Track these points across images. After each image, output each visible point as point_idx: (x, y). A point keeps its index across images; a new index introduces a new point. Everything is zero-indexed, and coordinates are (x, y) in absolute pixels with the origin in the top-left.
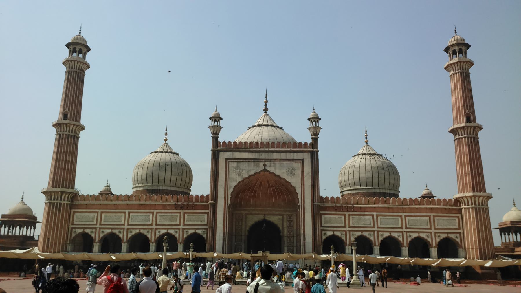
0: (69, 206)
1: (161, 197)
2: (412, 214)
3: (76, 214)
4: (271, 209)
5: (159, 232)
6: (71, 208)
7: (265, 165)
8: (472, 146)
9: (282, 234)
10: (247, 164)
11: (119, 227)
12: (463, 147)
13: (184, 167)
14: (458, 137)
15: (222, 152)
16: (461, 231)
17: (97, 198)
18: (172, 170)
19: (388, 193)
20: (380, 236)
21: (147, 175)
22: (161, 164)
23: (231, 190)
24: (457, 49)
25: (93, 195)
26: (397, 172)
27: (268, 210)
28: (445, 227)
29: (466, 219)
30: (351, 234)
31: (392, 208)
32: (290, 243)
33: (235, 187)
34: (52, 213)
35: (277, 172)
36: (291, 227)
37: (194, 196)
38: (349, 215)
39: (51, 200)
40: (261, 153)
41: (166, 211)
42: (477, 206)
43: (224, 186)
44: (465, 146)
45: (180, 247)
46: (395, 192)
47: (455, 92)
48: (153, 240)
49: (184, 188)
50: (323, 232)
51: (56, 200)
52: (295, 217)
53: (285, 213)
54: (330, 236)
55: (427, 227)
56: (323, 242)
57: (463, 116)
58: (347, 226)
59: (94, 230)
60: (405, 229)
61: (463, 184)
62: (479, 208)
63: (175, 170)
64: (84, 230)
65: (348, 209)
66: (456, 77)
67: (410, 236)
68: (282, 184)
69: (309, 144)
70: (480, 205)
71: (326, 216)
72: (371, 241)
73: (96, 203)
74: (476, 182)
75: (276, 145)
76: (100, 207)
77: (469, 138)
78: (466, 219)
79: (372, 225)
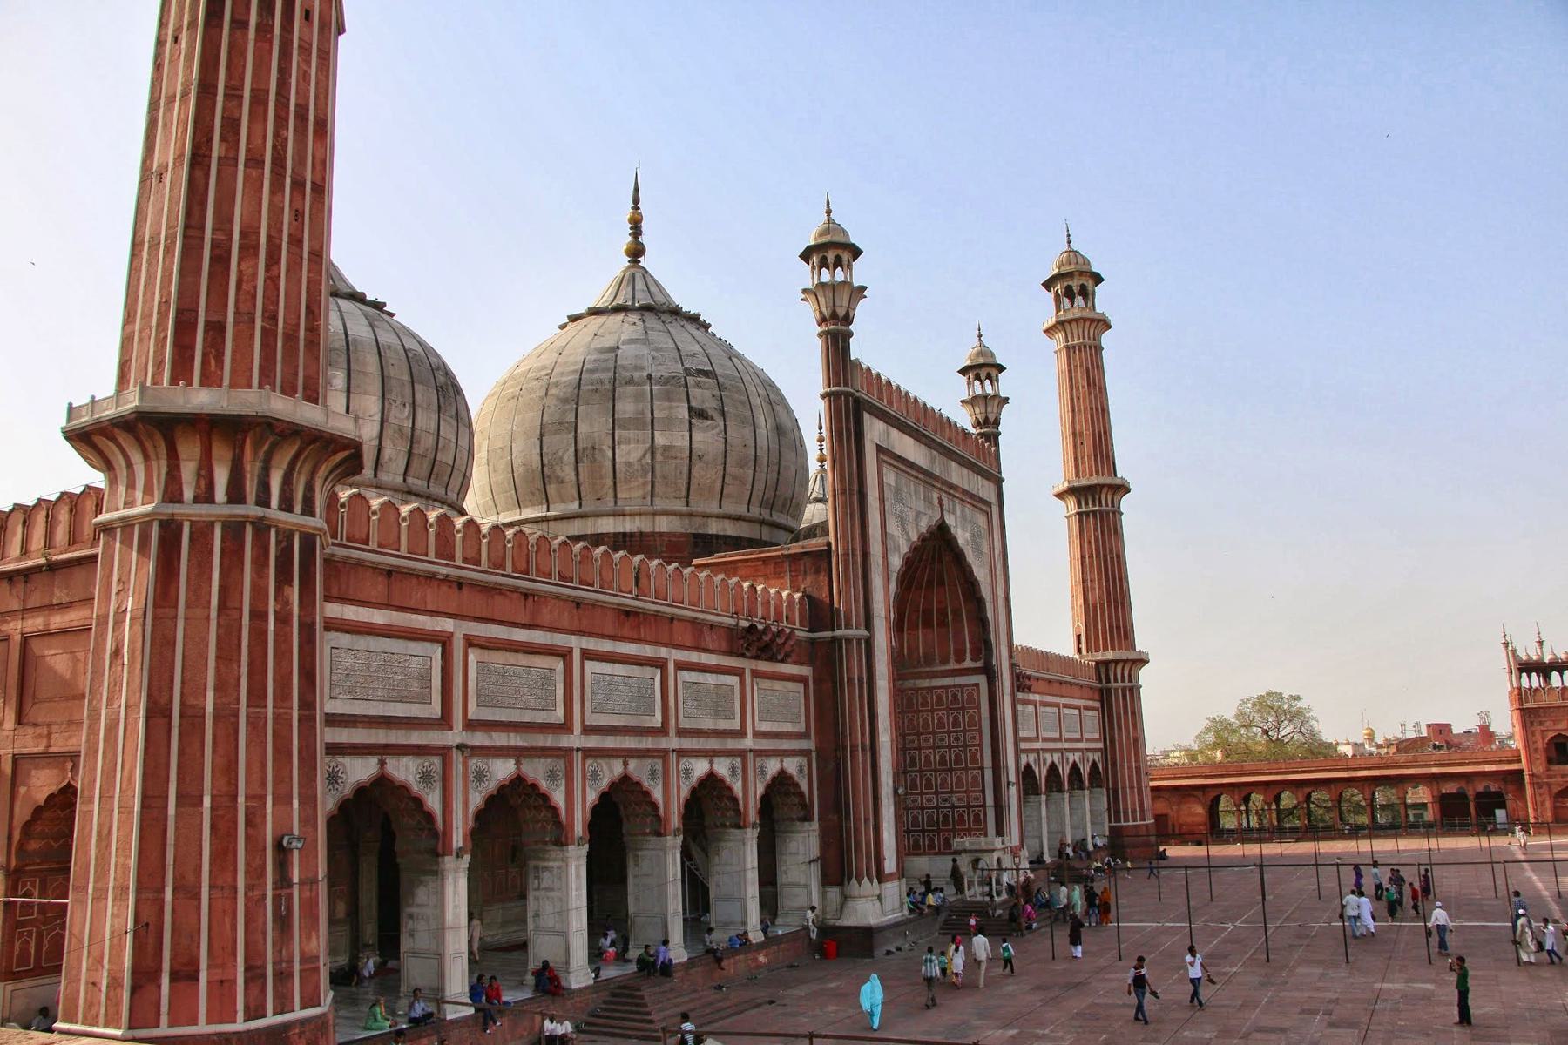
12: (1110, 535)
16: (1100, 745)
17: (438, 535)
21: (382, 422)
23: (893, 586)
24: (1089, 284)
34: (283, 619)
39: (267, 504)
40: (935, 453)
47: (1090, 394)
51: (298, 508)
59: (437, 761)
64: (382, 763)
66: (1091, 355)
73: (443, 570)
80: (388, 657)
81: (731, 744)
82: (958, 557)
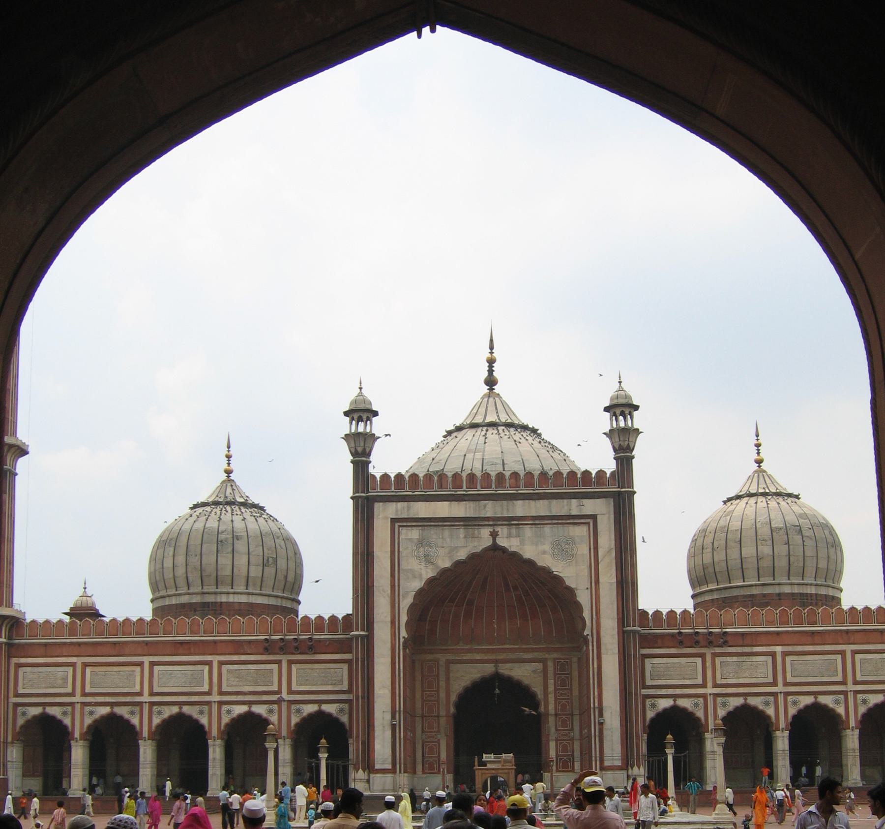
0: (5, 651)
1: (230, 623)
3: (21, 671)
4: (512, 646)
5: (229, 712)
6: (9, 657)
7: (494, 535)
9: (542, 709)
10: (447, 532)
11: (128, 699)
13: (280, 542)
15: (381, 504)
18: (250, 551)
19: (811, 595)
20: (789, 704)
21: (186, 565)
22: (222, 537)
23: (406, 602)
25: (60, 622)
26: (837, 539)
27: (506, 648)
30: (718, 702)
32: (564, 730)
33: (420, 593)
35: (528, 552)
36: (566, 691)
37: (313, 619)
38: (715, 655)
41: (243, 658)
43: (389, 592)
45: (284, 748)
46: (831, 592)
48: (215, 732)
49: (282, 598)
50: (648, 702)
52: (575, 666)
53: (549, 657)
54: (665, 710)
56: (650, 726)
58: (710, 684)
59: (69, 708)
60: (854, 684)
63: (257, 551)
64: (44, 709)
65: (710, 640)
67: (864, 702)
71: (656, 660)
72: (769, 717)
75: (522, 483)
76: (79, 649)
79: (770, 680)
80: (47, 673)
81: (265, 698)
82: (530, 563)
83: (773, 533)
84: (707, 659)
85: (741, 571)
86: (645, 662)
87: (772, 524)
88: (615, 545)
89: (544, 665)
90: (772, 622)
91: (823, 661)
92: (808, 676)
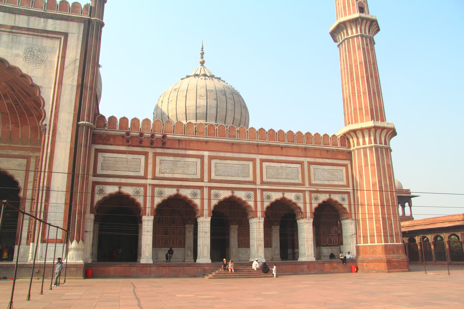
2: (274, 158)
8: (368, 50)
9: (21, 194)
12: (355, 52)
14: (346, 37)
16: (350, 189)
28: (326, 183)
29: (360, 167)
30: (155, 191)
31: (238, 144)
38: (155, 154)
42: (378, 144)
44: (358, 49)
50: (97, 188)
53: (33, 155)
55: (296, 181)
57: (353, 5)
58: (150, 176)
61: (355, 109)
62: (382, 148)
67: (269, 197)
68: (27, 93)
69: (83, 7)
70: (382, 144)
71: (107, 155)
72: (195, 205)
74: (376, 107)
77: (364, 38)
78: (360, 167)
79: (199, 176)
83: (208, 92)
84: (149, 157)
85: (185, 114)
86: (98, 155)
87: (207, 88)
88: (80, 57)
89: (27, 161)
90: (202, 133)
91: (239, 166)
92: (228, 176)
